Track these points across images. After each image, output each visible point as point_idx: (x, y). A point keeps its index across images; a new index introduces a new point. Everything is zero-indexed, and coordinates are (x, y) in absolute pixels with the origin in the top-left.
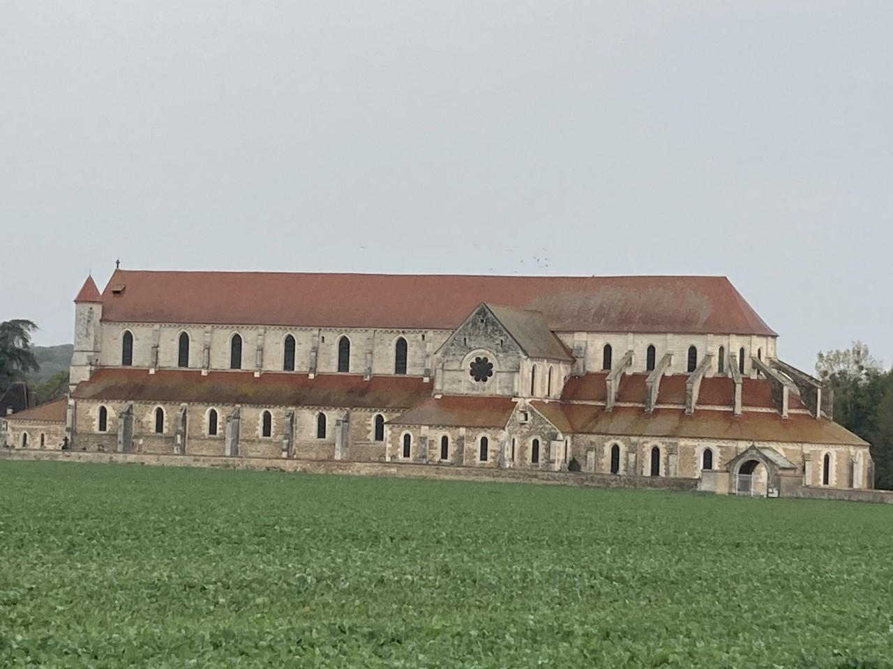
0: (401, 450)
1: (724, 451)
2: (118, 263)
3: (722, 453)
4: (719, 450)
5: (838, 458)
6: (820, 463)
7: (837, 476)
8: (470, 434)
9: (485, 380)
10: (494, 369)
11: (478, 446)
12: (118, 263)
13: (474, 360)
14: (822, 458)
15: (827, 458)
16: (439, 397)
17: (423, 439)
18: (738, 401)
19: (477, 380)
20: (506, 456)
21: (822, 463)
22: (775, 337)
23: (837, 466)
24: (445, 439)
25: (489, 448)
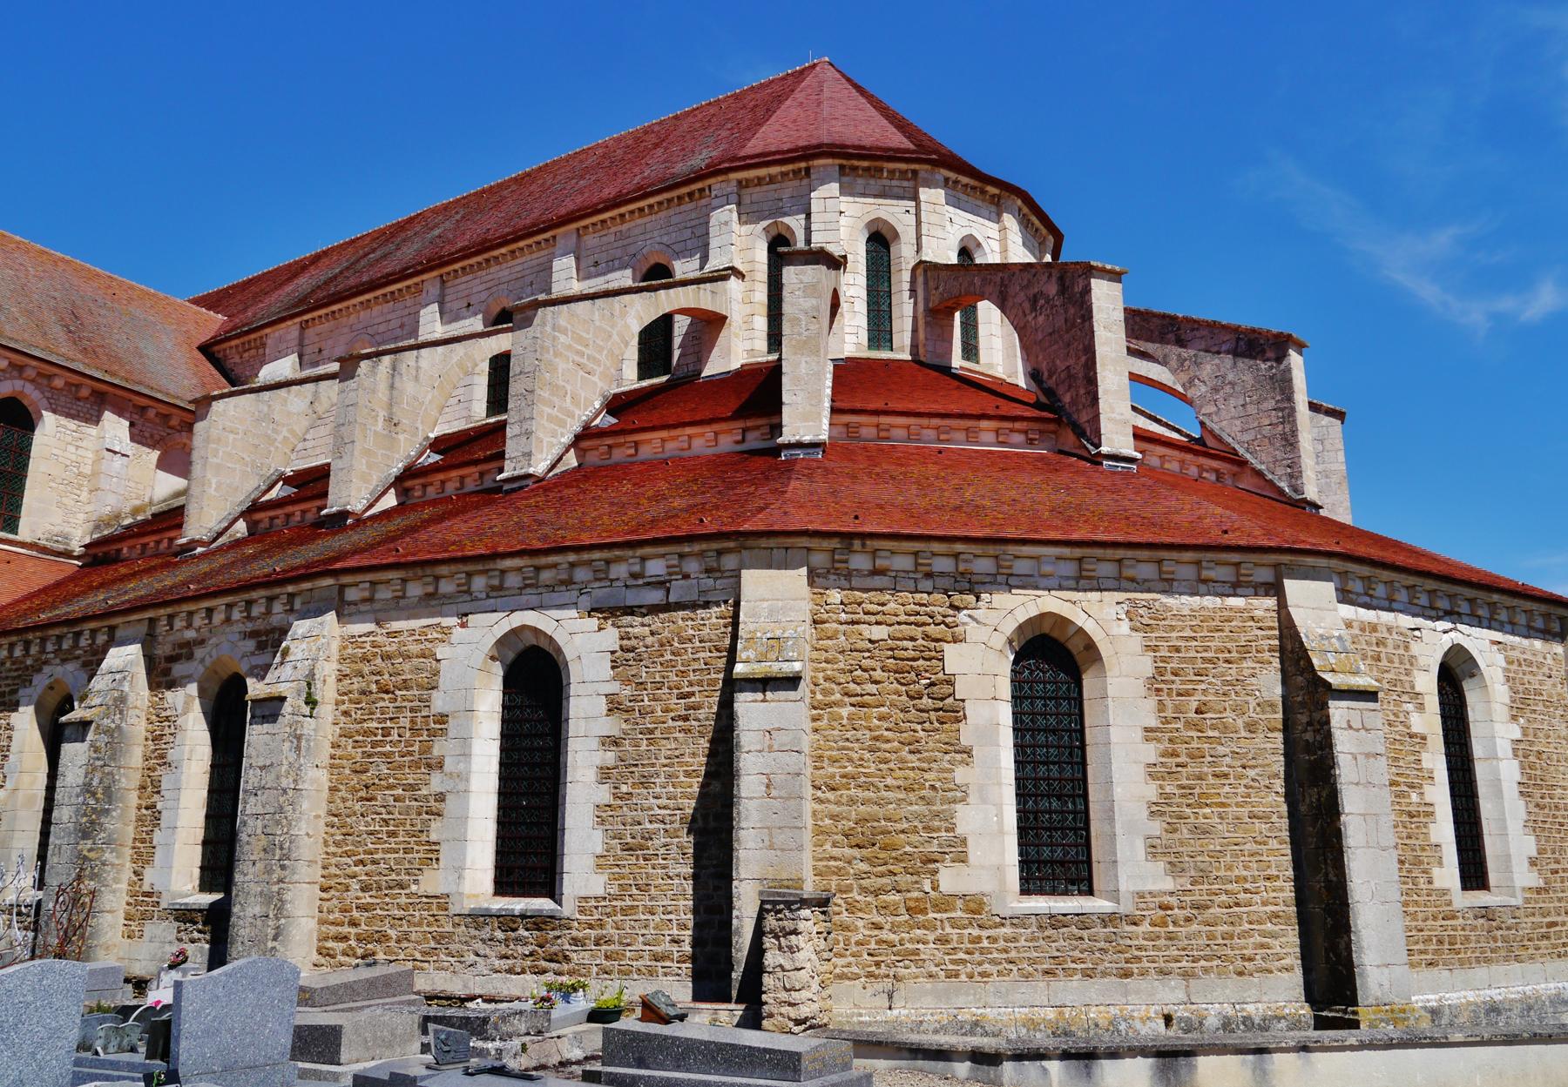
3: (624, 659)
7: (1534, 826)
21: (1428, 721)
23: (1520, 749)
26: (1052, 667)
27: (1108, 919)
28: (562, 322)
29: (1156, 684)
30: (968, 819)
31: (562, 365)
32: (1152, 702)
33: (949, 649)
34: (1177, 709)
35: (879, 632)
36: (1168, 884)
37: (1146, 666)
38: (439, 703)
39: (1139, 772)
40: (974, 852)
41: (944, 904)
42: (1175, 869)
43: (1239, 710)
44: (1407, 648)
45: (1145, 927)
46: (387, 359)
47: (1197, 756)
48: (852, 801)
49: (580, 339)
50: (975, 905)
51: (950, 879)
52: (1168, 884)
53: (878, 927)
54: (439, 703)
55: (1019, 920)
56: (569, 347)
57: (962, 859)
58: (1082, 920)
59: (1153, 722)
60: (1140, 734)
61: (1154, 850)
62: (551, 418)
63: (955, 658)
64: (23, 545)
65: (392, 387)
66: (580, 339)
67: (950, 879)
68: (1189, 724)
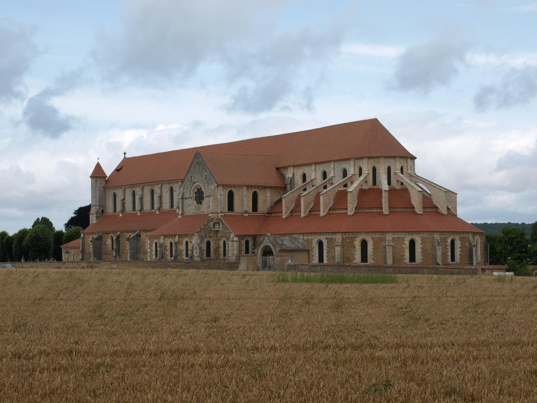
0: (154, 253)
1: (330, 241)
2: (125, 153)
5: (423, 242)
6: (404, 246)
8: (181, 239)
9: (201, 203)
10: (205, 195)
11: (183, 247)
12: (125, 153)
13: (196, 191)
14: (407, 243)
15: (453, 242)
16: (180, 217)
17: (161, 245)
18: (349, 206)
19: (198, 203)
20: (194, 254)
22: (413, 158)
24: (171, 243)
25: (189, 248)
26: (364, 244)
29: (373, 244)
30: (356, 256)
37: (372, 243)
38: (313, 246)
51: (354, 262)
61: (372, 259)
63: (355, 242)
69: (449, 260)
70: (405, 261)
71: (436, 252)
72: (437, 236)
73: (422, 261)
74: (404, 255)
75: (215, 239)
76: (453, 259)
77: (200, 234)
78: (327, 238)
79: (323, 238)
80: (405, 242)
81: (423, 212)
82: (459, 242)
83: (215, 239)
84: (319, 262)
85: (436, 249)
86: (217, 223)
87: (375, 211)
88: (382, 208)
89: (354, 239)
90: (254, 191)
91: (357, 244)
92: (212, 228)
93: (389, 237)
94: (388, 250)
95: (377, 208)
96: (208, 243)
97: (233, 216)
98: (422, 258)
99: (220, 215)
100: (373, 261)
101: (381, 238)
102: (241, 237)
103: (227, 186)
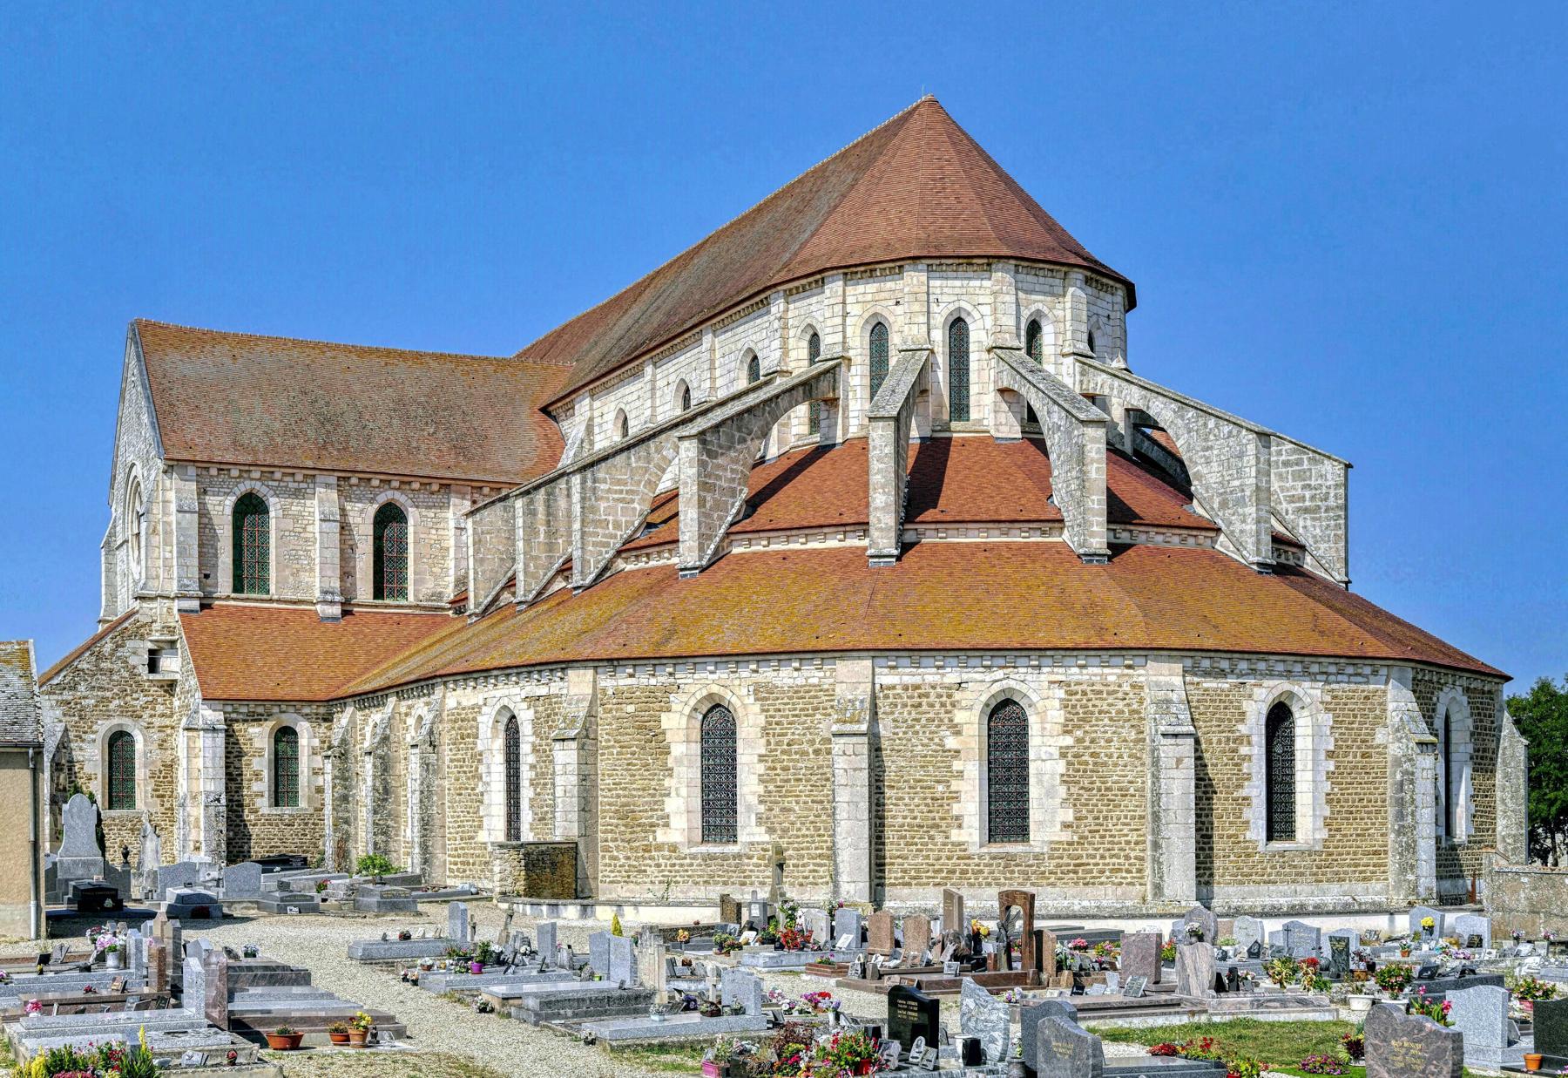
3: (536, 723)
4: (530, 714)
5: (1077, 716)
6: (951, 743)
14: (971, 720)
27: (738, 856)
28: (601, 475)
30: (672, 805)
31: (603, 505)
32: (763, 741)
33: (664, 716)
34: (777, 744)
35: (630, 709)
36: (766, 838)
37: (762, 720)
38: (480, 747)
39: (755, 779)
40: (673, 821)
41: (659, 848)
42: (771, 830)
43: (812, 742)
44: (950, 696)
45: (755, 860)
46: (543, 490)
47: (785, 769)
48: (618, 796)
49: (619, 482)
50: (673, 848)
51: (661, 836)
52: (766, 838)
53: (628, 858)
54: (480, 747)
55: (694, 857)
56: (609, 491)
57: (667, 825)
58: (725, 857)
59: (763, 752)
60: (756, 759)
61: (760, 820)
62: (595, 544)
63: (667, 721)
64: (410, 607)
65: (548, 507)
66: (619, 482)
67: (661, 836)
68: (783, 752)
69: (1258, 831)
70: (955, 835)
71: (1156, 778)
72: (1166, 677)
73: (1066, 836)
74: (955, 797)
75: (157, 721)
76: (1279, 821)
77: (67, 695)
78: (532, 700)
79: (513, 694)
80: (960, 717)
81: (1110, 546)
82: (1327, 719)
83: (157, 721)
84: (509, 836)
85: (1156, 762)
86: (173, 643)
87: (832, 543)
88: (863, 526)
89: (659, 700)
90: (383, 498)
91: (679, 727)
92: (143, 670)
93: (851, 678)
94: (841, 763)
95: (843, 527)
96: (119, 744)
97: (253, 615)
98: (1069, 815)
99: (176, 605)
100: (761, 835)
101: (808, 688)
102: (240, 708)
103: (223, 467)
